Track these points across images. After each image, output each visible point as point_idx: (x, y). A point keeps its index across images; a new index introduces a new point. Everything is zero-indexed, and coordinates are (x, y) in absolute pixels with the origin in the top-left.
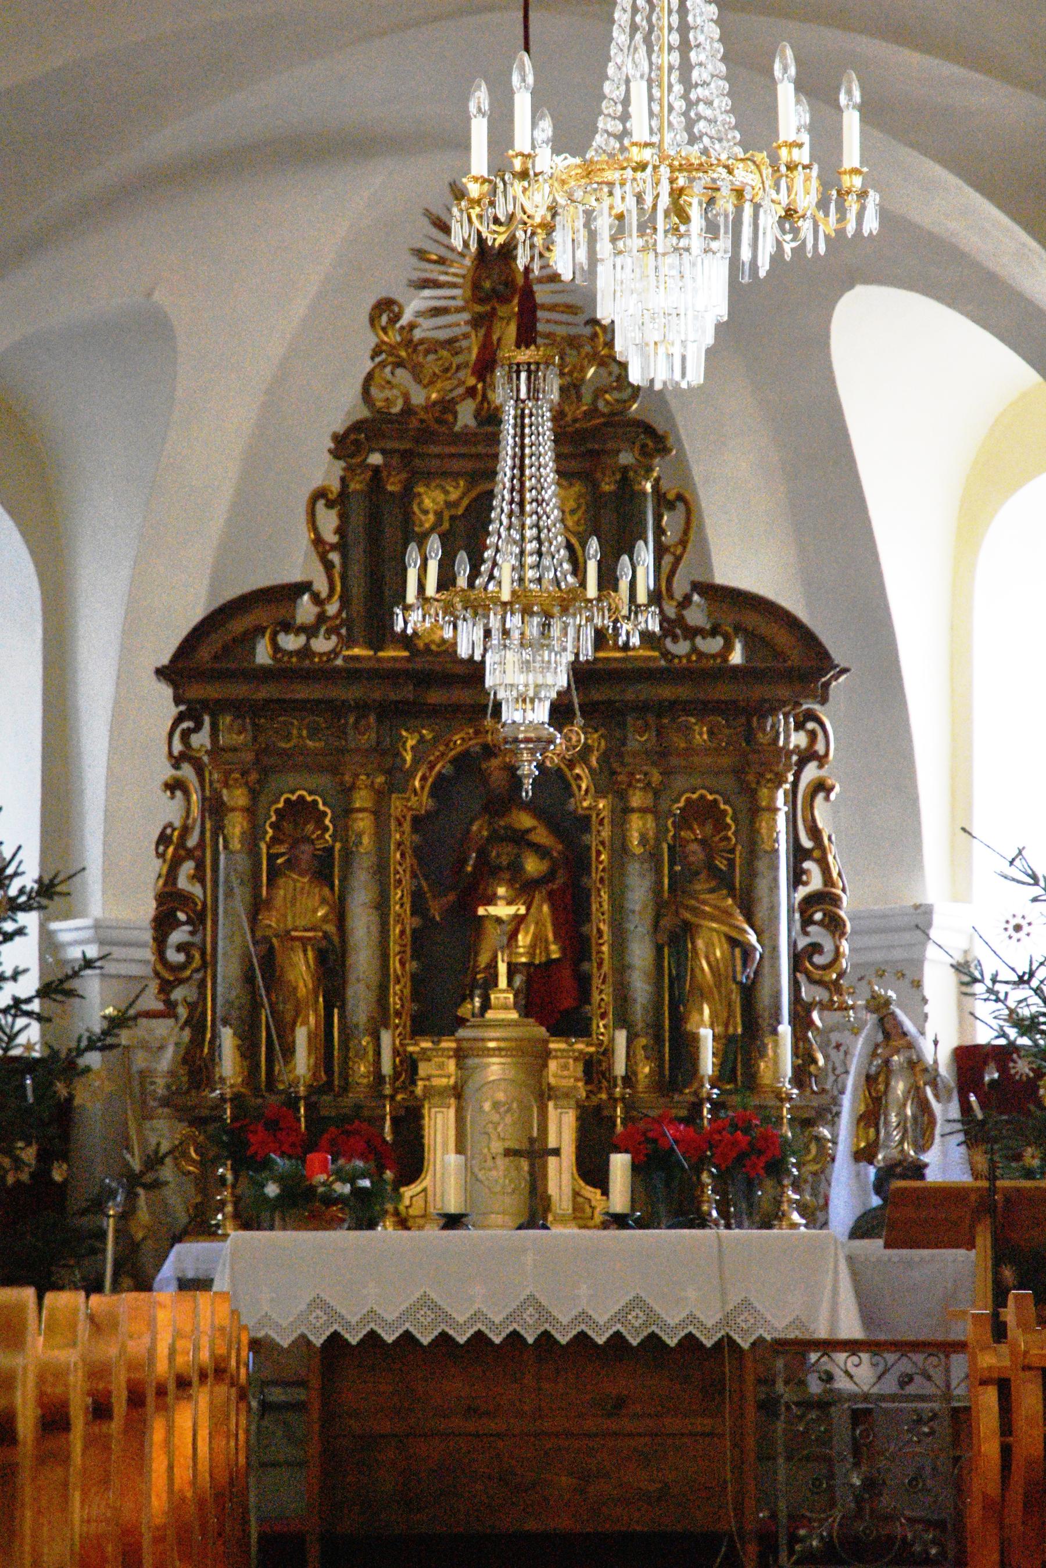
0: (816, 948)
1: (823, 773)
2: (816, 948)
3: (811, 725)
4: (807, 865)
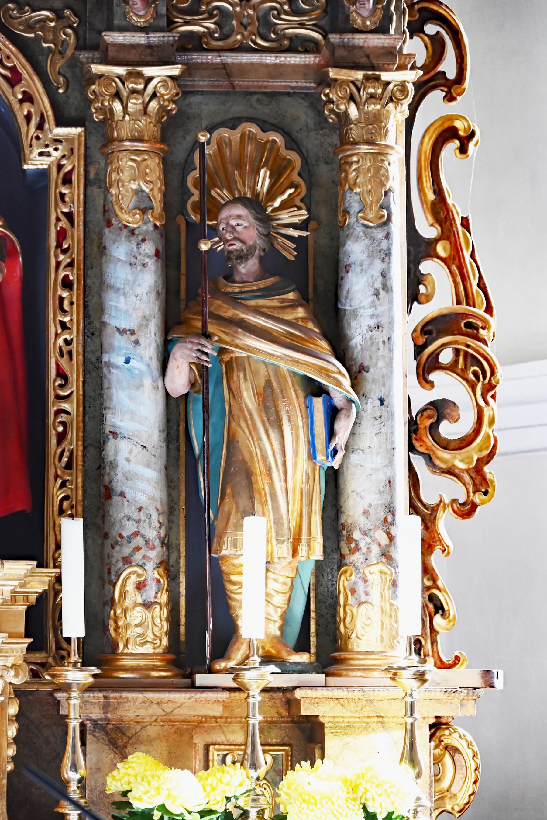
0: (440, 409)
1: (452, 108)
2: (440, 409)
3: (431, 29)
4: (425, 267)
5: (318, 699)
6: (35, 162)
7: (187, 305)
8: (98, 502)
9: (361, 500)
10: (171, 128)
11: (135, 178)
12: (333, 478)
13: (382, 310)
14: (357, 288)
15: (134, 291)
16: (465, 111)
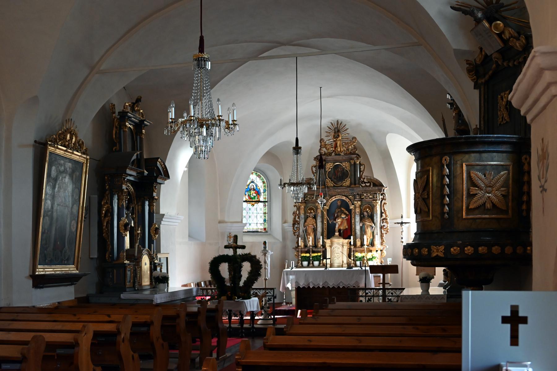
0: (384, 226)
5: (371, 248)
6: (351, 208)
7: (362, 220)
8: (355, 234)
9: (375, 233)
10: (360, 206)
11: (358, 210)
12: (373, 233)
13: (378, 218)
14: (375, 218)
15: (358, 219)
16: (386, 202)
